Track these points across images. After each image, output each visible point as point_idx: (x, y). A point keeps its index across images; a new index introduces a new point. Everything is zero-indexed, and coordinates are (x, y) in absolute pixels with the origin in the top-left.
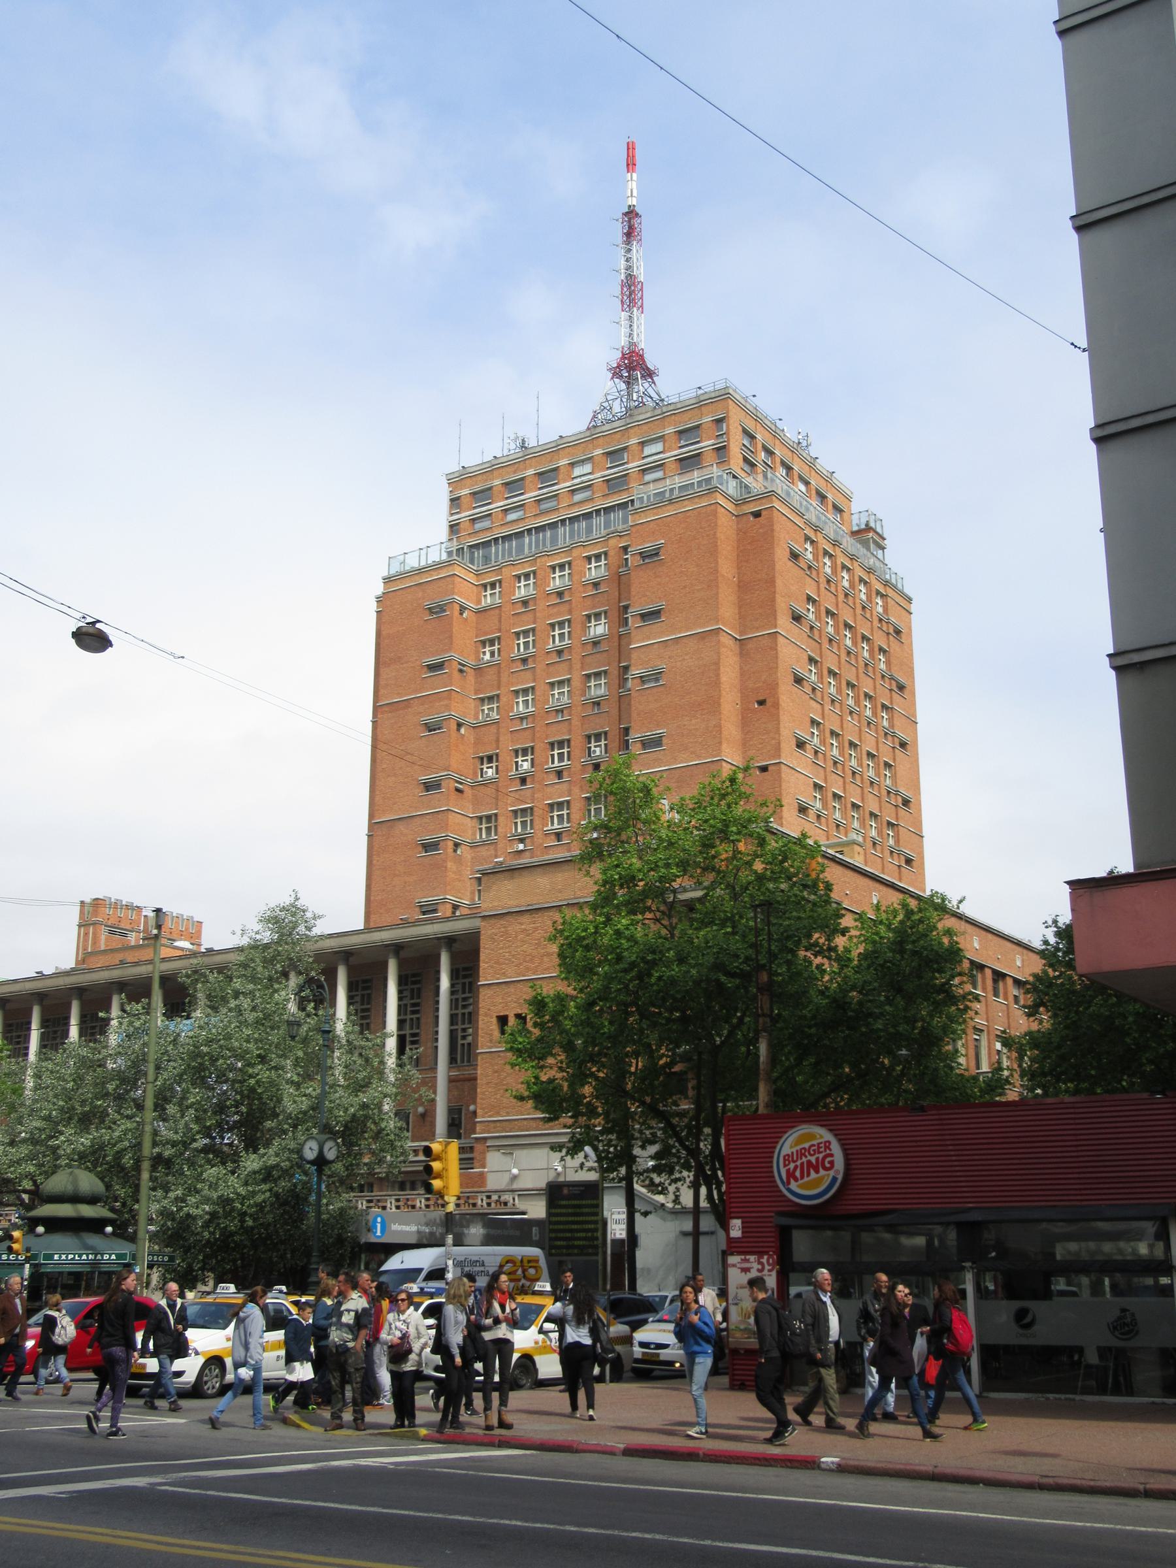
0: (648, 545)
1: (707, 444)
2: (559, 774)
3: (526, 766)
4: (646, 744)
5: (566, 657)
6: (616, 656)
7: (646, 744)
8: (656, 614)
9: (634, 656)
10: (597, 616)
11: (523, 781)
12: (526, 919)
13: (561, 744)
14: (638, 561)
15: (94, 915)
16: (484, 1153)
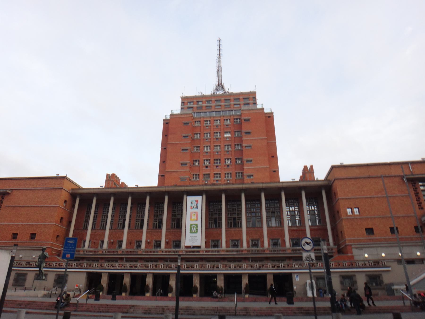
0: (246, 118)
1: (251, 102)
2: (217, 166)
3: (208, 163)
4: (248, 161)
5: (219, 140)
6: (238, 141)
7: (248, 161)
8: (249, 133)
9: (243, 141)
10: (227, 132)
11: (207, 167)
12: (353, 181)
13: (217, 160)
14: (244, 121)
15: (112, 179)
16: (351, 249)
